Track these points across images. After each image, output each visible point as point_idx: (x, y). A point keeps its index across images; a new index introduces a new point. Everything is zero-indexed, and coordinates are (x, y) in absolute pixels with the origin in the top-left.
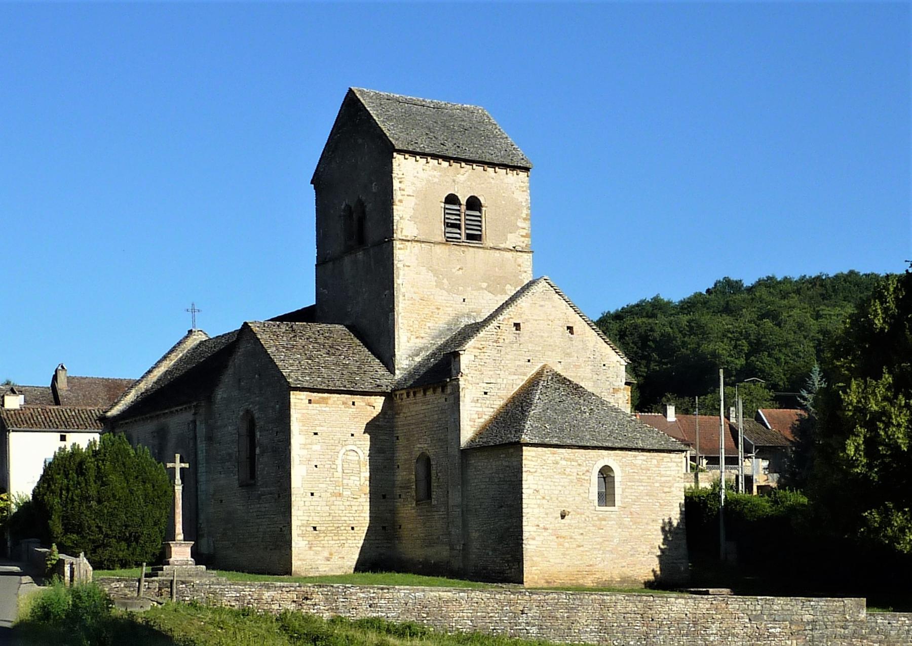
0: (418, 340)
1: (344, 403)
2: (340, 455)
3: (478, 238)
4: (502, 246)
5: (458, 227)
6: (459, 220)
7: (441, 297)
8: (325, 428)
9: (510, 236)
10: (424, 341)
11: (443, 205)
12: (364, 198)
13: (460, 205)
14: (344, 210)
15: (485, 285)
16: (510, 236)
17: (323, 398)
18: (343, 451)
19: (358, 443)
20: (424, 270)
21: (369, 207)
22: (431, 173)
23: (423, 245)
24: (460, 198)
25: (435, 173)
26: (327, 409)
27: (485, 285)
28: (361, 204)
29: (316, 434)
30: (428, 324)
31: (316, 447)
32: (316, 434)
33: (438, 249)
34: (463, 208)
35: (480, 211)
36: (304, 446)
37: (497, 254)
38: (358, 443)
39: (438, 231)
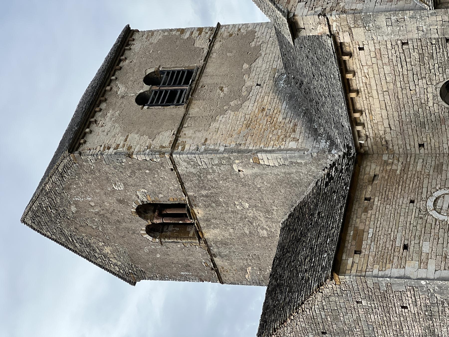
0: (298, 130)
1: (366, 210)
2: (441, 217)
3: (190, 73)
4: (206, 51)
5: (174, 93)
6: (166, 91)
7: (250, 107)
8: (399, 235)
9: (198, 44)
10: (299, 124)
11: (146, 107)
12: (135, 206)
13: (150, 91)
14: (154, 237)
15: (246, 66)
16: (197, 45)
17: (354, 238)
18: (435, 214)
19: (424, 196)
20: (215, 125)
21: (142, 196)
22: (107, 119)
23: (185, 125)
24: (142, 91)
25: (109, 114)
26: (371, 231)
27: (246, 66)
28: (143, 210)
29: (406, 247)
30: (280, 119)
31: (426, 247)
32: (406, 247)
33: (195, 110)
34: (155, 88)
35: (162, 72)
36: (423, 263)
37: (214, 55)
38: (424, 196)
39: (176, 111)
